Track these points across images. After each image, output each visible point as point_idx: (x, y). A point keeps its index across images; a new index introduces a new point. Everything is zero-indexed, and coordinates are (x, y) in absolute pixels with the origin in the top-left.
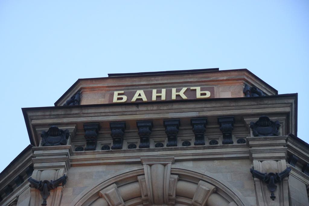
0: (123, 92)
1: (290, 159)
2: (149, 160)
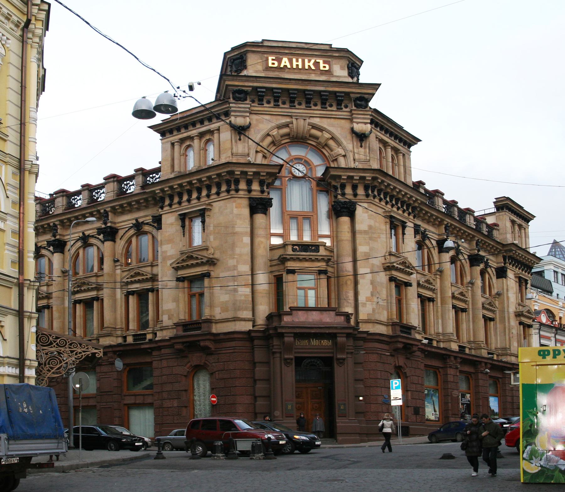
0: (274, 58)
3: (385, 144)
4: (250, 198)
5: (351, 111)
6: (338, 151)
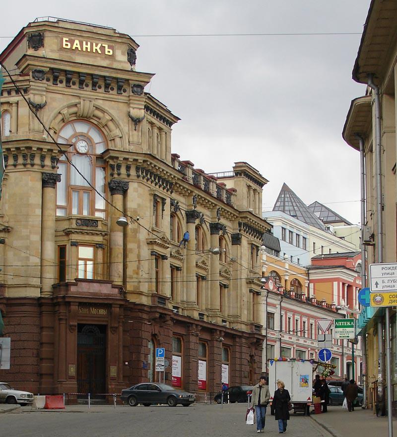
0: (68, 39)
1: (147, 108)
3: (152, 124)
4: (43, 173)
5: (129, 96)
6: (116, 132)
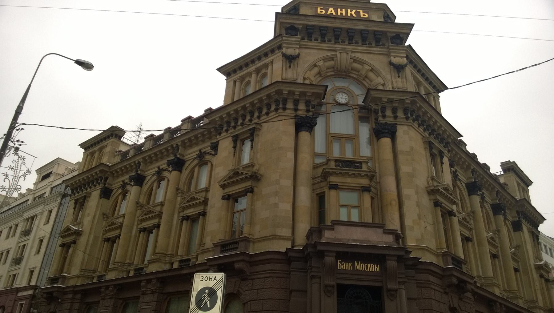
1: (407, 57)
2: (339, 50)
5: (388, 48)
